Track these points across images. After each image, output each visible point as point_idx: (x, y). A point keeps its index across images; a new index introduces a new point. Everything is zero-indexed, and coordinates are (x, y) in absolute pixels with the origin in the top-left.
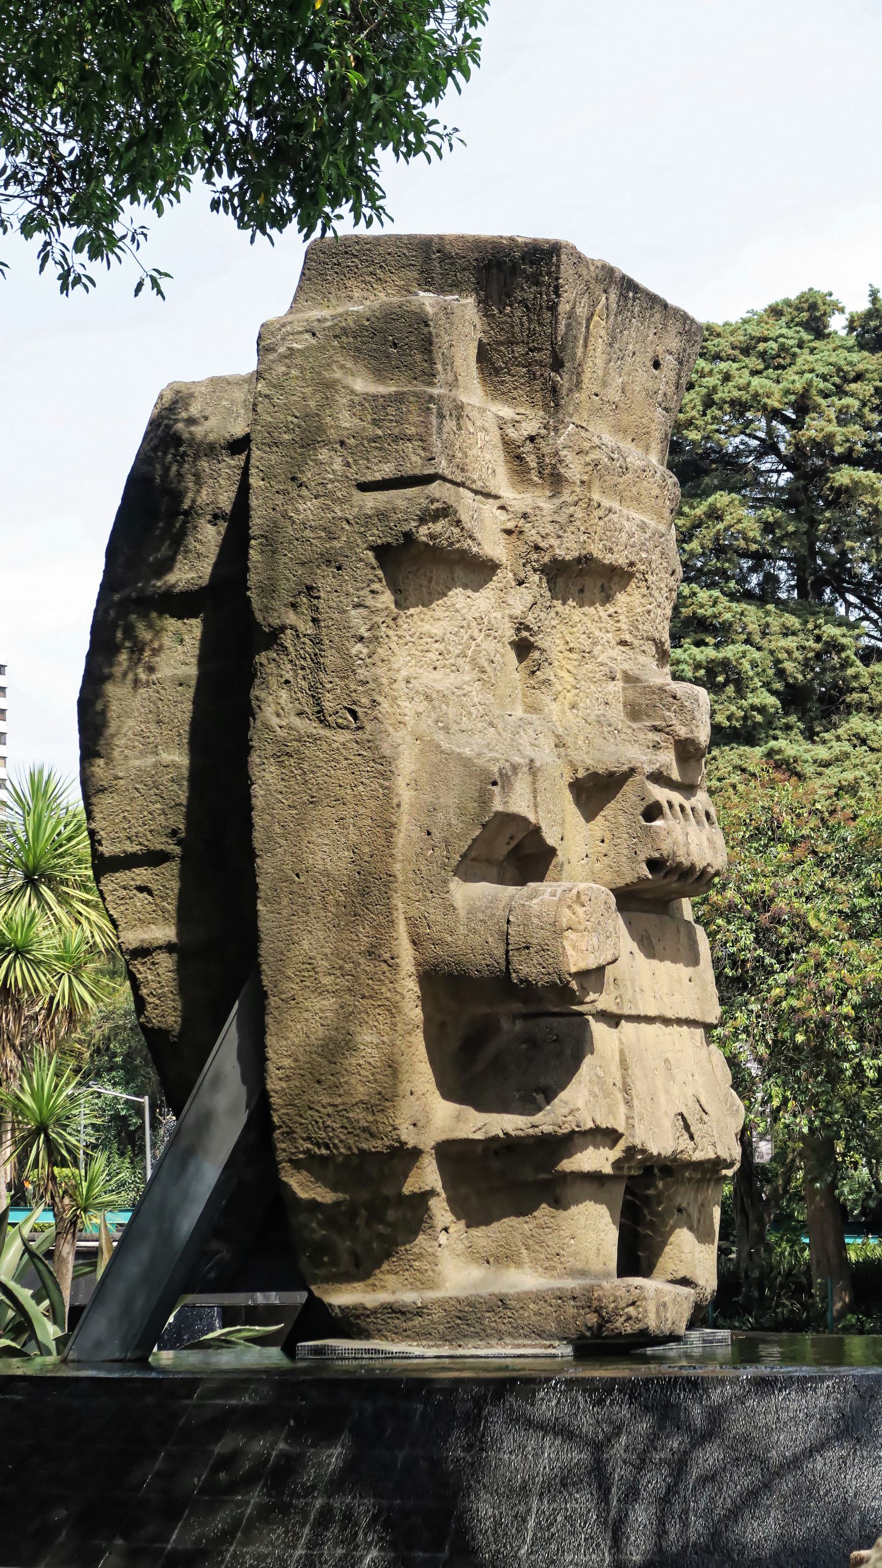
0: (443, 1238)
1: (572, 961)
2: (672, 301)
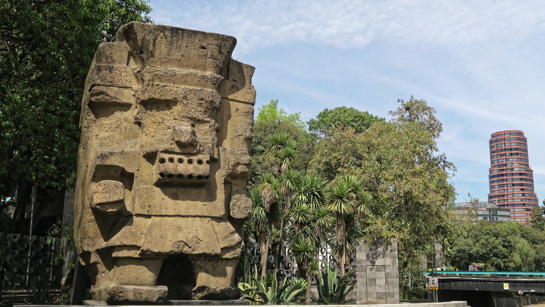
0: (103, 275)
1: (95, 201)
2: (207, 31)
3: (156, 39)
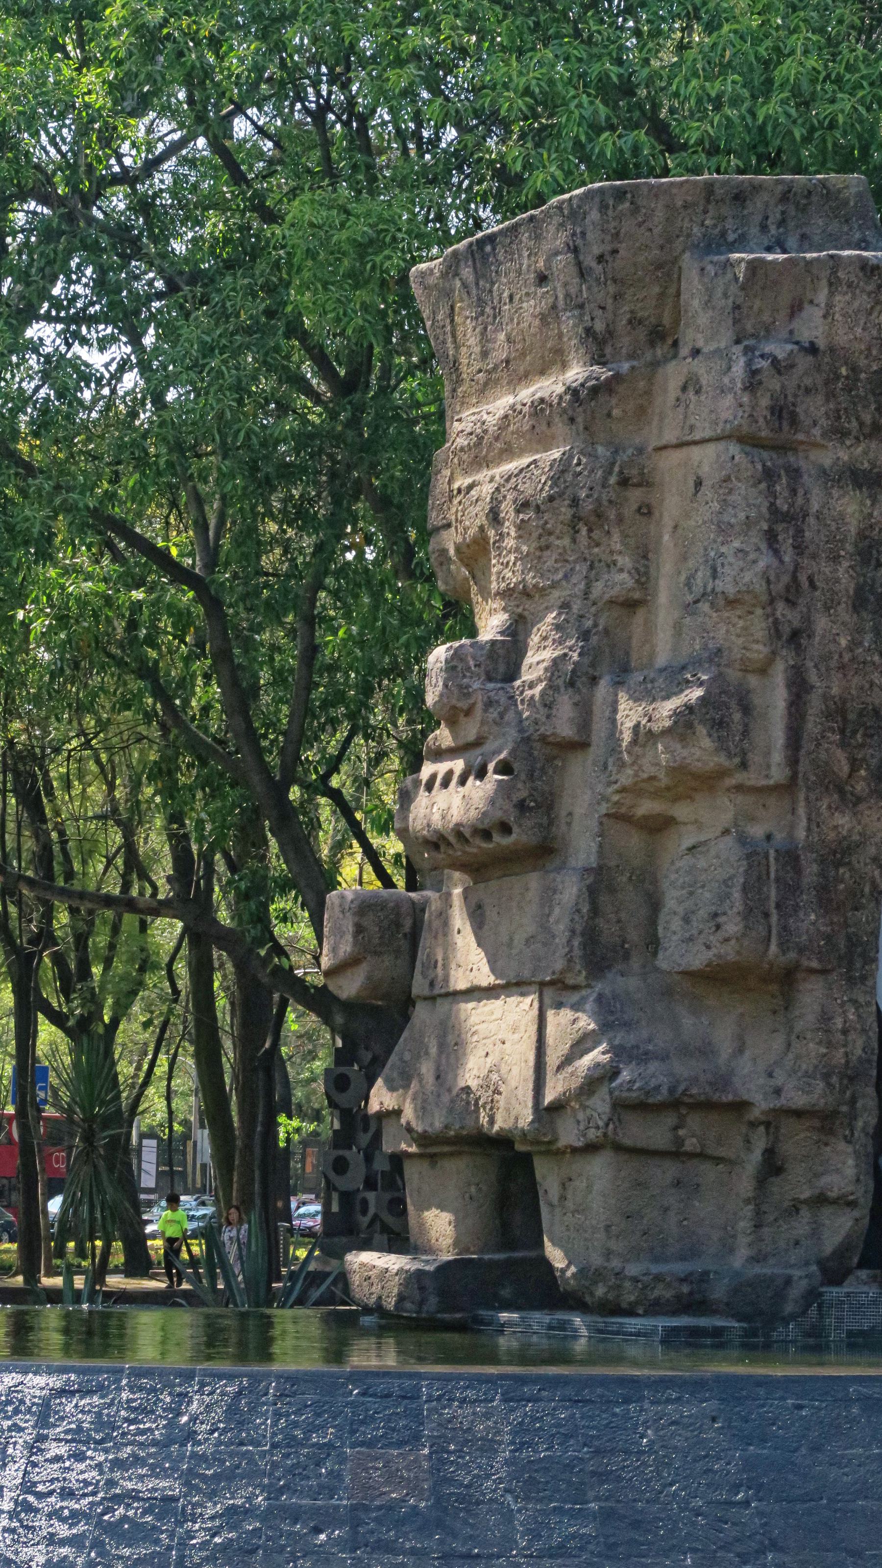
3: (452, 308)
